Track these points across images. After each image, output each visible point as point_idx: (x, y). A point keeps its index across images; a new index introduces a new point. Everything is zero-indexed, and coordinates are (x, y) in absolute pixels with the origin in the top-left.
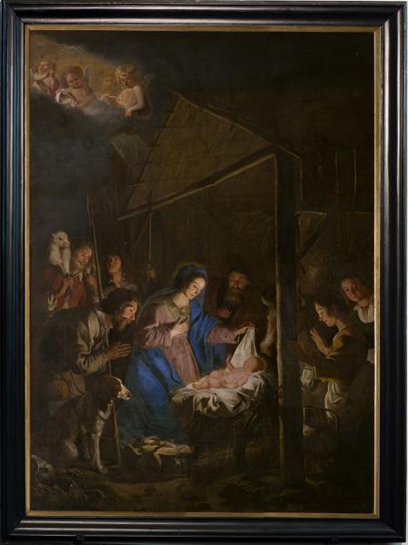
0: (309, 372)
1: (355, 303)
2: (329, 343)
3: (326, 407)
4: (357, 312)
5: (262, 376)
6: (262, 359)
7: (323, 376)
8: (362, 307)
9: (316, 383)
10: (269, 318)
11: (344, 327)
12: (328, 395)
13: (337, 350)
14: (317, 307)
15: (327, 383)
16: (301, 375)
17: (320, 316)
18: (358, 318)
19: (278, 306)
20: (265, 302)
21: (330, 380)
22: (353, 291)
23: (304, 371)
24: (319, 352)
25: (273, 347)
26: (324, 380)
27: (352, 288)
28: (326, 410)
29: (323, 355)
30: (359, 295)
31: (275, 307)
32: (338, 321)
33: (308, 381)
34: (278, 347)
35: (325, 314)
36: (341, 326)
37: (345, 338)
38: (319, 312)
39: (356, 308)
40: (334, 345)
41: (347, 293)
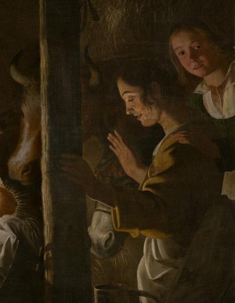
0: (105, 218)
1: (199, 80)
2: (145, 160)
3: (140, 287)
4: (200, 98)
5: (11, 226)
6: (11, 191)
7: (133, 225)
8: (212, 88)
9: (119, 239)
10: (25, 109)
11: (176, 126)
12: (144, 264)
13: (158, 175)
14: (122, 87)
15: (141, 239)
16: (88, 223)
17: (128, 105)
18: (204, 109)
19: (44, 84)
20: (18, 78)
21: (148, 234)
22: (194, 56)
23: (96, 215)
24: (127, 177)
25: (33, 167)
26: (135, 233)
27: (191, 49)
28: (140, 294)
29: (134, 184)
30: (206, 63)
31: (39, 85)
32: (164, 115)
33: (104, 236)
34: (44, 168)
35: (138, 100)
36: (170, 126)
37: (177, 150)
38: (126, 97)
39: (199, 89)
40: (156, 162)
41: (181, 57)
